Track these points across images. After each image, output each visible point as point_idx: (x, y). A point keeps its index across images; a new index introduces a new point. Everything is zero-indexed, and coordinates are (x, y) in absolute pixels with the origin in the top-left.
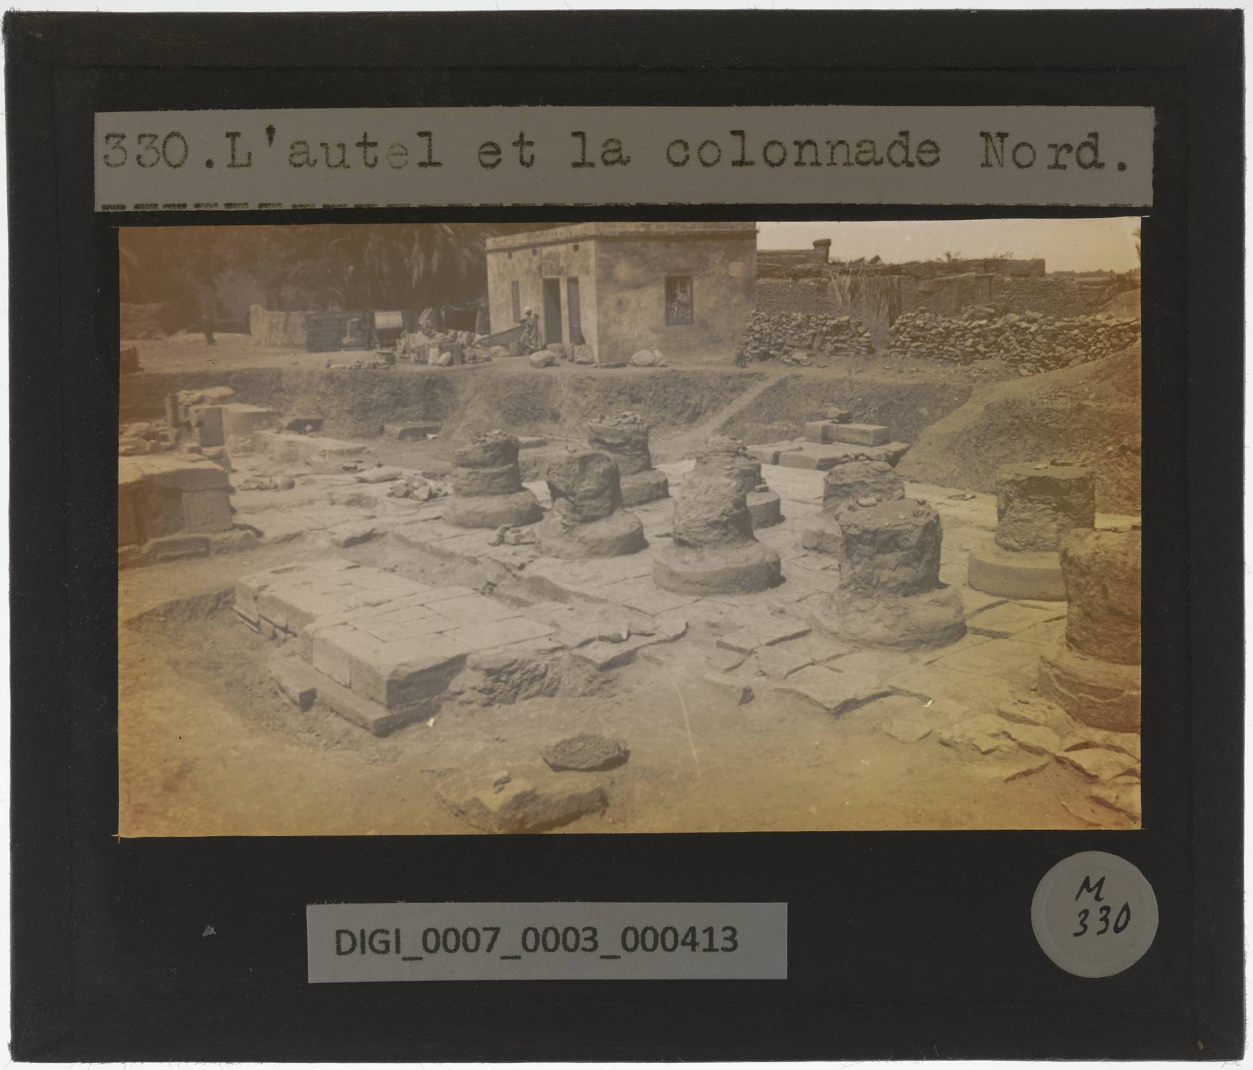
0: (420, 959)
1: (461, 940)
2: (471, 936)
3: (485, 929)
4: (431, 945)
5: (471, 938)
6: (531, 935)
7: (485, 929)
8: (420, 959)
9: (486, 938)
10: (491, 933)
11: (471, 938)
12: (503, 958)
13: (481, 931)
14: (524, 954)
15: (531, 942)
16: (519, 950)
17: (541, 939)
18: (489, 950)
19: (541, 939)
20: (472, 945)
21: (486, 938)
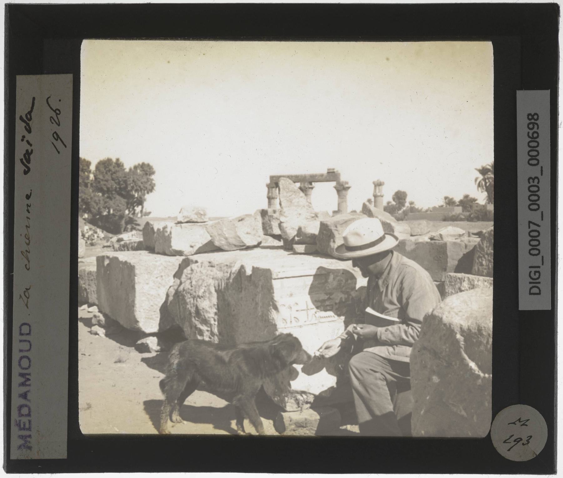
0: (543, 257)
1: (533, 238)
2: (532, 234)
3: (529, 227)
4: (537, 252)
5: (534, 234)
6: (532, 207)
7: (529, 228)
8: (543, 257)
9: (533, 227)
10: (531, 224)
11: (534, 234)
12: (542, 220)
13: (531, 229)
14: (541, 210)
15: (535, 207)
16: (539, 212)
17: (534, 202)
18: (538, 226)
19: (534, 202)
20: (535, 234)
21: (533, 227)
